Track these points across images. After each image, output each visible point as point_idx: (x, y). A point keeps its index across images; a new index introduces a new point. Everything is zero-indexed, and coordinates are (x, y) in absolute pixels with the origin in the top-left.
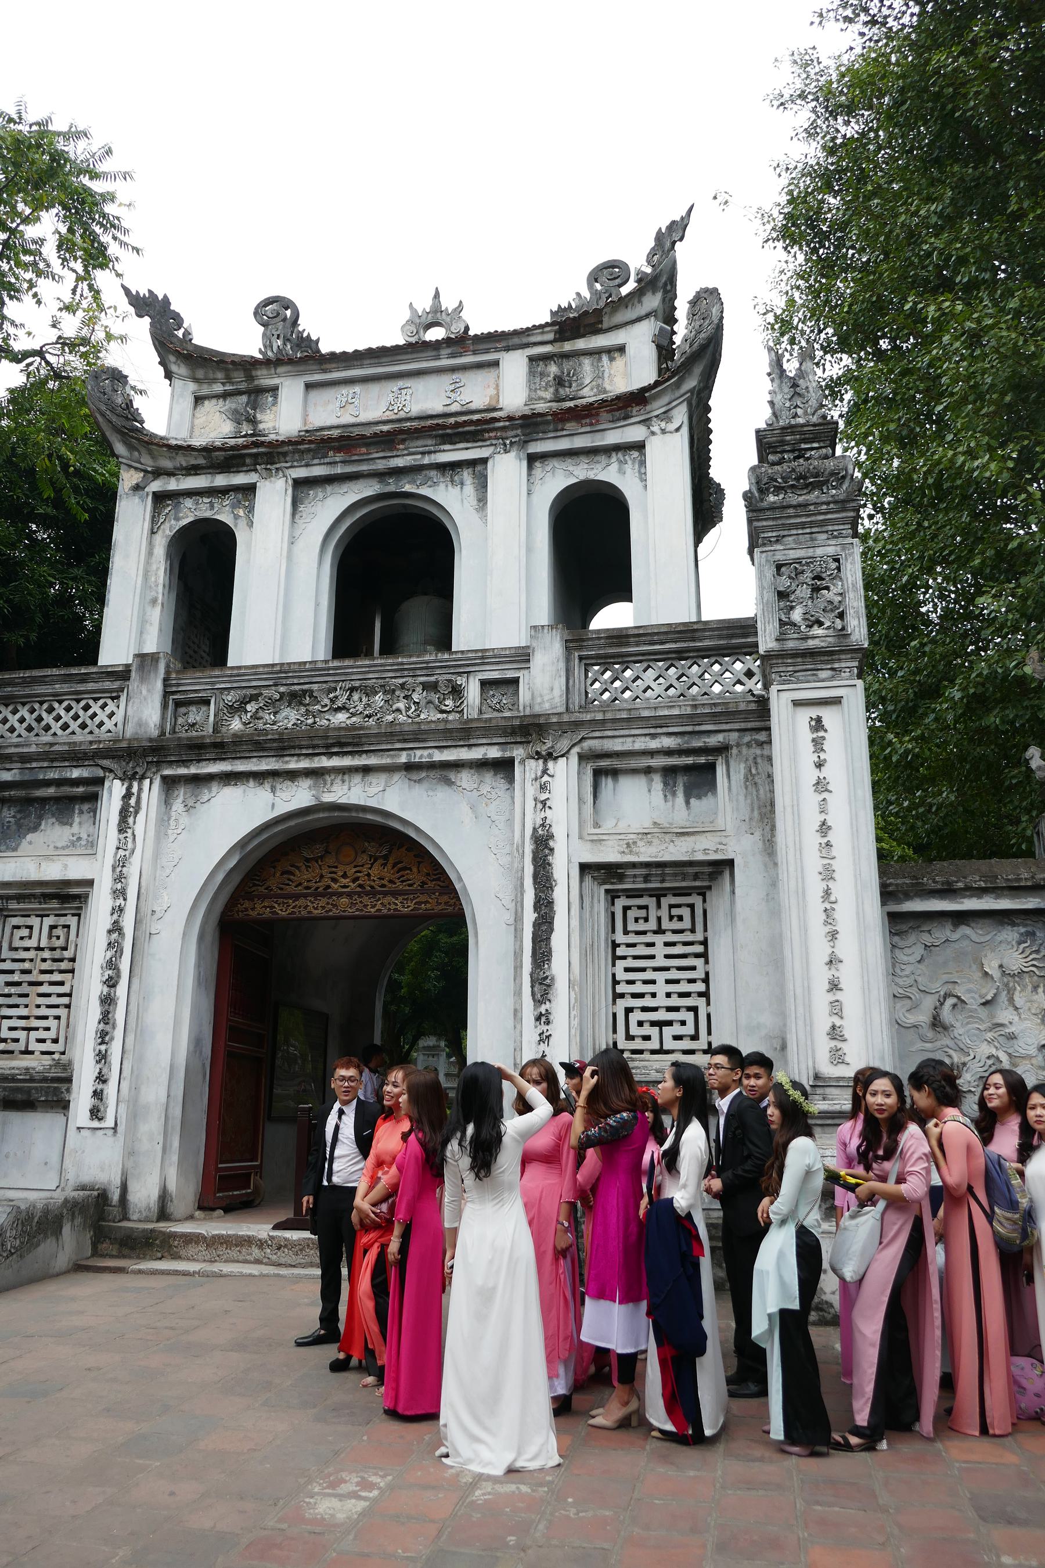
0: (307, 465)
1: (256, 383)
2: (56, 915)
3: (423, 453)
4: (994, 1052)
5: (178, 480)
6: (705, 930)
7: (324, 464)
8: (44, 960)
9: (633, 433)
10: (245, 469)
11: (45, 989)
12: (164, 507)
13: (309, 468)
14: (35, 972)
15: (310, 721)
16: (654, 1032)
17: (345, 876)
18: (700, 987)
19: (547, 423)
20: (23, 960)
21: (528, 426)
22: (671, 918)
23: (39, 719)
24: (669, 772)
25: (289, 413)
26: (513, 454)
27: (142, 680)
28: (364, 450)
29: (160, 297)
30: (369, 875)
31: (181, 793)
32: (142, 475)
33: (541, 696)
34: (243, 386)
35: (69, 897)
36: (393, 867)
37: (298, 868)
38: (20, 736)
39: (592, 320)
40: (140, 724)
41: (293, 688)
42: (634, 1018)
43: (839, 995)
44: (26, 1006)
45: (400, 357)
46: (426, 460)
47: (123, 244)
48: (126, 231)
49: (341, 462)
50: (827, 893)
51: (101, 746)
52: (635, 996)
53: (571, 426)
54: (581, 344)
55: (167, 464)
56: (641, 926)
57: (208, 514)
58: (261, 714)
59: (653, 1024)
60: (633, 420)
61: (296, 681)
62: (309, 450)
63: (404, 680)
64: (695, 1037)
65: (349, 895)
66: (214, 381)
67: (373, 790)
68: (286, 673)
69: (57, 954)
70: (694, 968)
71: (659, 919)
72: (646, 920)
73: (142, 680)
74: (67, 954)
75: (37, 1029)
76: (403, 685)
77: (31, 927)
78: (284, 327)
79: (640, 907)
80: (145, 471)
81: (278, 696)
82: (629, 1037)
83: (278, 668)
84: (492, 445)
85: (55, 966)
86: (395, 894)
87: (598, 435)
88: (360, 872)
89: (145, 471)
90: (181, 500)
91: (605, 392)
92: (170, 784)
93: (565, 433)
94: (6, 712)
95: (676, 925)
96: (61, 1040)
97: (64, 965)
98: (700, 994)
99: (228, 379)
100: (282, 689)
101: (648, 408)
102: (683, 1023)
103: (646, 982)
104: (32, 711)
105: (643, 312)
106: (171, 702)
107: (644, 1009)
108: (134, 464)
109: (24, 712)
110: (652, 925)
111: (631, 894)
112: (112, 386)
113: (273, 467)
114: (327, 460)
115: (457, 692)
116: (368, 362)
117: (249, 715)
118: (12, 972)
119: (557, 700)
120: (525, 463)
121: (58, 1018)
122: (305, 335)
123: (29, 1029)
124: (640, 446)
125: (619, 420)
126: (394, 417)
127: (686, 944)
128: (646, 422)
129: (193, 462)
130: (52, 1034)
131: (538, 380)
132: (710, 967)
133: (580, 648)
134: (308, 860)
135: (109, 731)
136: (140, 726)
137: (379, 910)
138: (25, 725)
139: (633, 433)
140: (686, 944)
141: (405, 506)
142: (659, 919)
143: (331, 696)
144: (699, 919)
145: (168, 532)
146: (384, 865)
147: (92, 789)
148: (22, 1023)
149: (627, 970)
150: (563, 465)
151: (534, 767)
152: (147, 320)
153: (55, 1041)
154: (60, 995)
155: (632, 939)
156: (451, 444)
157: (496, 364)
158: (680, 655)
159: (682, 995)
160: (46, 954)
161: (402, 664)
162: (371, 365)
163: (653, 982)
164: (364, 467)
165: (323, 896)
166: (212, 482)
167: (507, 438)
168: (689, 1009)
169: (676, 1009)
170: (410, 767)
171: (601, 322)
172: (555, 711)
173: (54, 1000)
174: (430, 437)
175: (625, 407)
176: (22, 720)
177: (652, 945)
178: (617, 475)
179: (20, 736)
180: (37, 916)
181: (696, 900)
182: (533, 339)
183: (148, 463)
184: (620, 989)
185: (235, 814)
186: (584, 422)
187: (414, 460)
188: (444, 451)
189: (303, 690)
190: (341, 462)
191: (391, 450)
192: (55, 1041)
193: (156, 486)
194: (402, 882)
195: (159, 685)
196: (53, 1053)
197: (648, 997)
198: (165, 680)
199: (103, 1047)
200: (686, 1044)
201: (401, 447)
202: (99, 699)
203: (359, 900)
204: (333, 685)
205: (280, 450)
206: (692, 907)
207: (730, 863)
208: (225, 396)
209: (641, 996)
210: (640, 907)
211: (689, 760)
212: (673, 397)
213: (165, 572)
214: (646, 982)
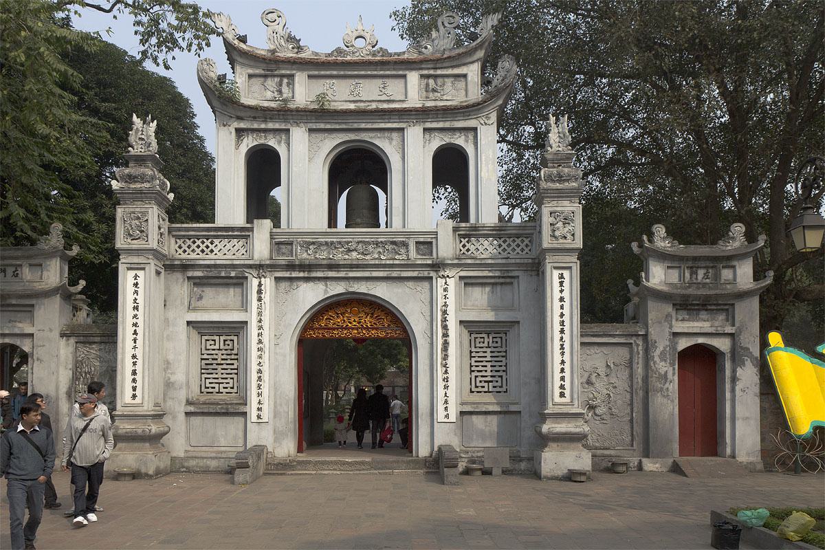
4: (608, 392)
8: (223, 355)
9: (471, 123)
11: (225, 366)
14: (219, 360)
16: (486, 385)
17: (354, 321)
18: (504, 368)
20: (212, 354)
21: (421, 114)
25: (303, 92)
31: (284, 285)
35: (238, 328)
42: (478, 379)
43: (564, 374)
44: (217, 374)
50: (562, 338)
52: (478, 371)
56: (482, 345)
59: (485, 382)
64: (501, 387)
65: (357, 329)
67: (370, 287)
69: (229, 352)
70: (501, 361)
71: (488, 342)
72: (483, 343)
74: (235, 352)
75: (223, 383)
77: (215, 340)
82: (476, 387)
85: (229, 357)
86: (377, 329)
95: (495, 345)
96: (235, 388)
97: (233, 357)
98: (504, 371)
102: (497, 381)
103: (483, 366)
104: (203, 242)
105: (476, 59)
107: (482, 376)
110: (486, 344)
118: (208, 359)
121: (233, 378)
123: (219, 383)
124: (475, 129)
130: (231, 385)
132: (508, 361)
134: (338, 314)
139: (471, 123)
142: (488, 342)
147: (241, 281)
148: (216, 381)
149: (475, 361)
150: (441, 135)
151: (441, 282)
153: (232, 388)
154: (231, 369)
157: (404, 76)
159: (496, 371)
160: (224, 352)
163: (486, 366)
165: (345, 329)
168: (499, 376)
169: (494, 376)
173: (229, 371)
182: (423, 66)
184: (473, 369)
185: (310, 295)
192: (232, 388)
196: (231, 393)
197: (484, 372)
199: (260, 391)
200: (498, 389)
206: (501, 338)
207: (518, 322)
209: (481, 371)
214: (483, 366)
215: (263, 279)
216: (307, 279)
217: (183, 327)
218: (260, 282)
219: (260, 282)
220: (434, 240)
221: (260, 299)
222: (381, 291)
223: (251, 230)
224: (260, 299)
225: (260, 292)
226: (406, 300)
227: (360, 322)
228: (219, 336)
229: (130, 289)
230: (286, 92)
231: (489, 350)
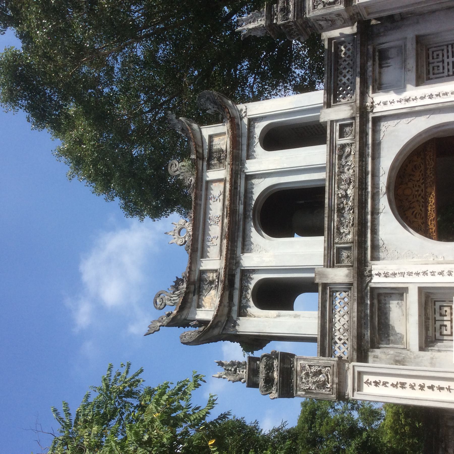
1: (196, 280)
2: (435, 314)
6: (443, 46)
22: (437, 58)
24: (381, 67)
30: (418, 181)
36: (414, 172)
37: (413, 212)
40: (347, 276)
46: (242, 199)
55: (226, 310)
56: (441, 68)
57: (250, 291)
60: (240, 123)
66: (192, 299)
71: (438, 62)
72: (438, 67)
79: (433, 69)
86: (426, 169)
87: (243, 135)
88: (416, 186)
92: (374, 258)
95: (441, 56)
105: (198, 130)
111: (428, 73)
115: (343, 147)
124: (250, 120)
126: (221, 221)
127: (448, 52)
128: (241, 118)
137: (433, 175)
140: (448, 52)
143: (340, 195)
144: (439, 48)
146: (413, 175)
147: (376, 296)
152: (161, 328)
155: (446, 70)
158: (336, 69)
170: (373, 159)
175: (235, 125)
177: (448, 64)
180: (435, 323)
181: (431, 51)
182: (201, 168)
191: (236, 211)
193: (234, 315)
194: (420, 166)
203: (428, 184)
210: (433, 69)
211: (377, 58)
215: (373, 273)
216: (375, 232)
217: (427, 355)
218: (376, 275)
219: (376, 275)
221: (394, 274)
222: (386, 162)
223: (325, 286)
224: (394, 274)
225: (386, 275)
226: (395, 139)
227: (419, 186)
228: (435, 320)
229: (381, 391)
230: (212, 276)
231: (446, 60)
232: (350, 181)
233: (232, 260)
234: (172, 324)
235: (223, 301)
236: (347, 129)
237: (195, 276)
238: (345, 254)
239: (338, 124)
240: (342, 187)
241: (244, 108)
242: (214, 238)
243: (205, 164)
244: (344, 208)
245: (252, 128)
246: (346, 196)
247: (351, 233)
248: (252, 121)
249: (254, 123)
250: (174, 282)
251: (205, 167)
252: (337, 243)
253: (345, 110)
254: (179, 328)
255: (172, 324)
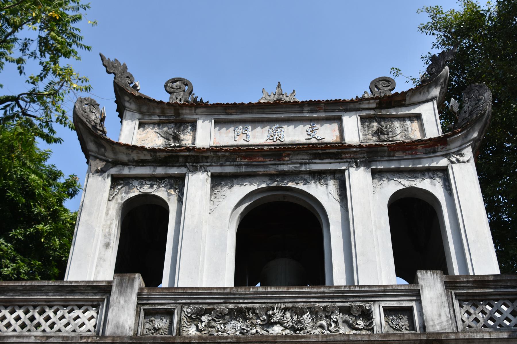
0: (221, 165)
1: (181, 117)
3: (301, 164)
5: (130, 168)
7: (233, 165)
10: (178, 164)
12: (118, 185)
13: (222, 168)
15: (254, 331)
19: (384, 151)
23: (32, 319)
26: (362, 169)
27: (121, 293)
28: (261, 159)
29: (122, 64)
32: (104, 163)
33: (433, 320)
34: (172, 119)
38: (14, 330)
39: (399, 98)
40: (117, 326)
41: (239, 305)
45: (278, 110)
46: (303, 168)
47: (81, 46)
48: (80, 38)
49: (245, 165)
51: (90, 340)
53: (398, 154)
54: (393, 112)
55: (124, 158)
58: (213, 323)
60: (438, 154)
61: (241, 301)
62: (224, 156)
63: (325, 304)
66: (153, 114)
68: (234, 294)
73: (121, 293)
76: (325, 308)
78: (184, 95)
80: (107, 161)
81: (226, 311)
83: (228, 291)
84: (347, 162)
87: (417, 161)
89: (107, 161)
90: (130, 181)
91: (410, 138)
93: (395, 158)
94: (5, 312)
99: (163, 114)
100: (231, 306)
101: (448, 147)
104: (26, 313)
105: (429, 97)
106: (142, 311)
108: (100, 156)
109: (20, 312)
112: (90, 109)
113: (199, 165)
114: (235, 163)
115: (367, 315)
116: (257, 111)
117: (204, 324)
119: (445, 323)
120: (370, 174)
122: (198, 100)
125: (429, 153)
128: (447, 156)
129: (142, 157)
131: (366, 129)
133: (455, 288)
135: (89, 331)
136: (118, 327)
138: (20, 322)
141: (285, 196)
143: (270, 312)
145: (119, 201)
152: (113, 75)
156: (320, 159)
161: (324, 292)
162: (258, 113)
164: (261, 170)
166: (154, 171)
167: (357, 159)
171: (405, 100)
172: (444, 331)
174: (307, 154)
175: (434, 145)
176: (18, 319)
178: (430, 186)
179: (14, 330)
182: (363, 106)
183: (110, 156)
186: (407, 152)
187: (295, 167)
188: (315, 163)
189: (247, 308)
190: (245, 165)
193: (114, 171)
195: (134, 298)
198: (139, 294)
201: (287, 159)
202: (83, 305)
204: (271, 305)
205: (204, 155)
208: (159, 124)
212: (463, 142)
213: (116, 226)
220: (414, 304)
232: (298, 329)
233: (197, 159)
234: (118, 89)
235: (135, 151)
236: (404, 322)
237: (187, 114)
238: (161, 323)
239: (414, 304)
240: (288, 315)
241: (465, 159)
242: (247, 136)
243: (372, 113)
244: (245, 319)
245: (431, 174)
246: (269, 324)
247: (199, 333)
248: (443, 173)
249: (440, 177)
250: (201, 99)
251: (364, 113)
252: (182, 310)
253: (440, 316)
254: (115, 102)
255: (118, 89)
